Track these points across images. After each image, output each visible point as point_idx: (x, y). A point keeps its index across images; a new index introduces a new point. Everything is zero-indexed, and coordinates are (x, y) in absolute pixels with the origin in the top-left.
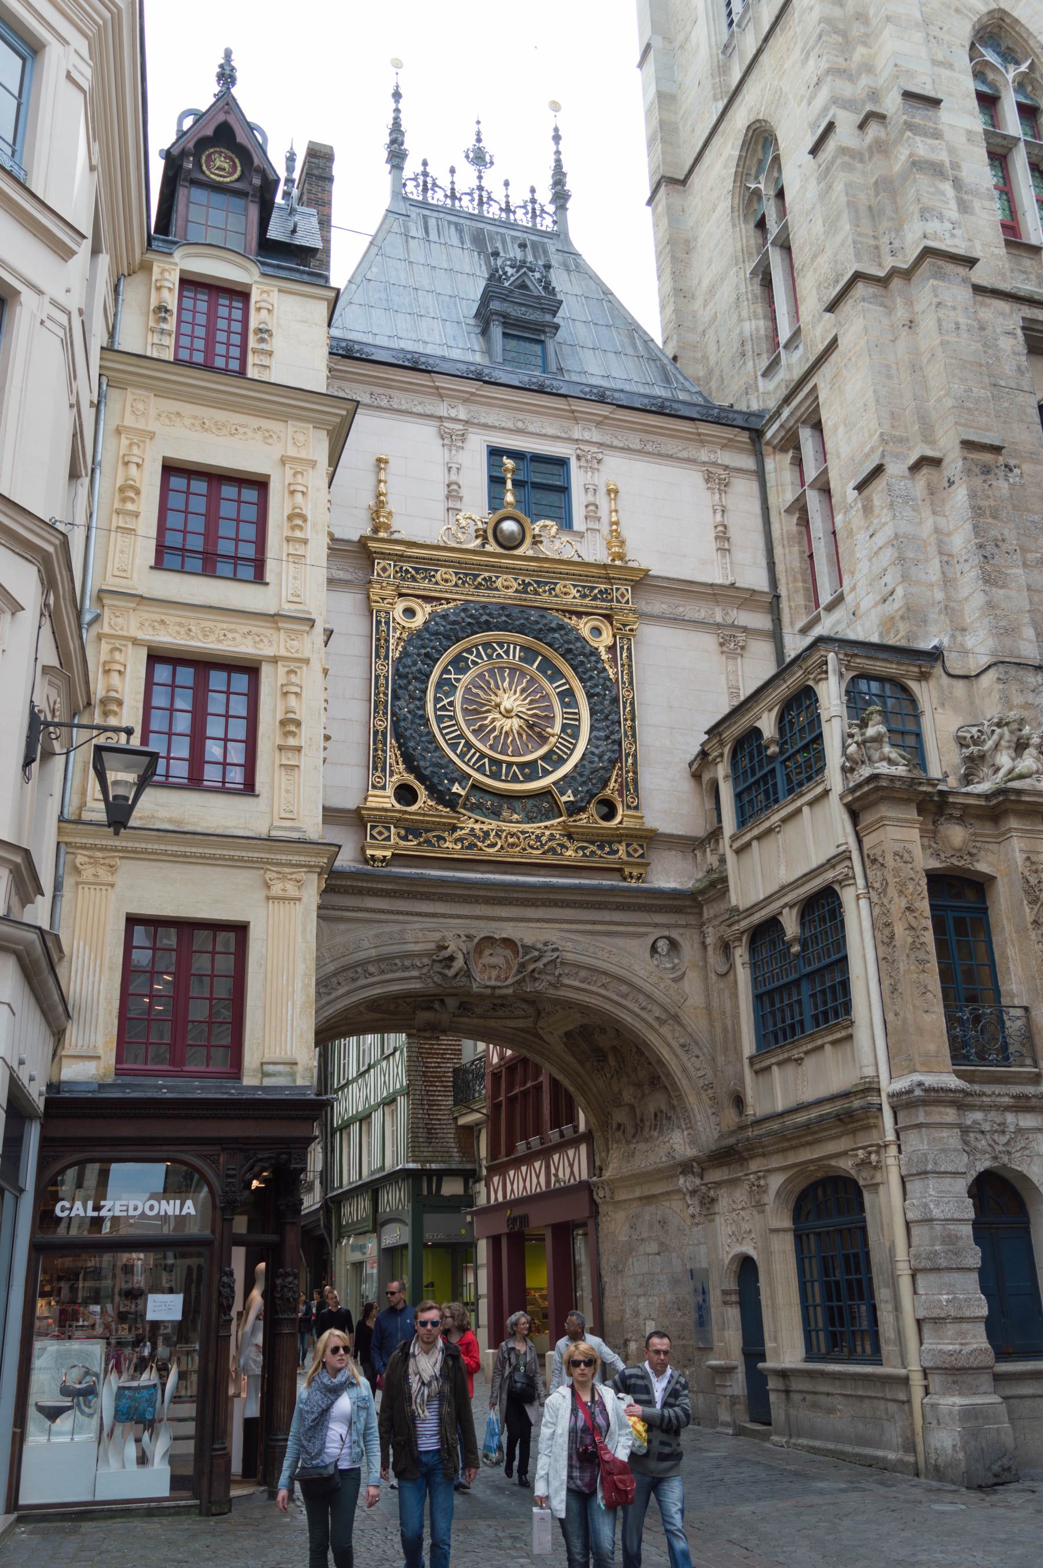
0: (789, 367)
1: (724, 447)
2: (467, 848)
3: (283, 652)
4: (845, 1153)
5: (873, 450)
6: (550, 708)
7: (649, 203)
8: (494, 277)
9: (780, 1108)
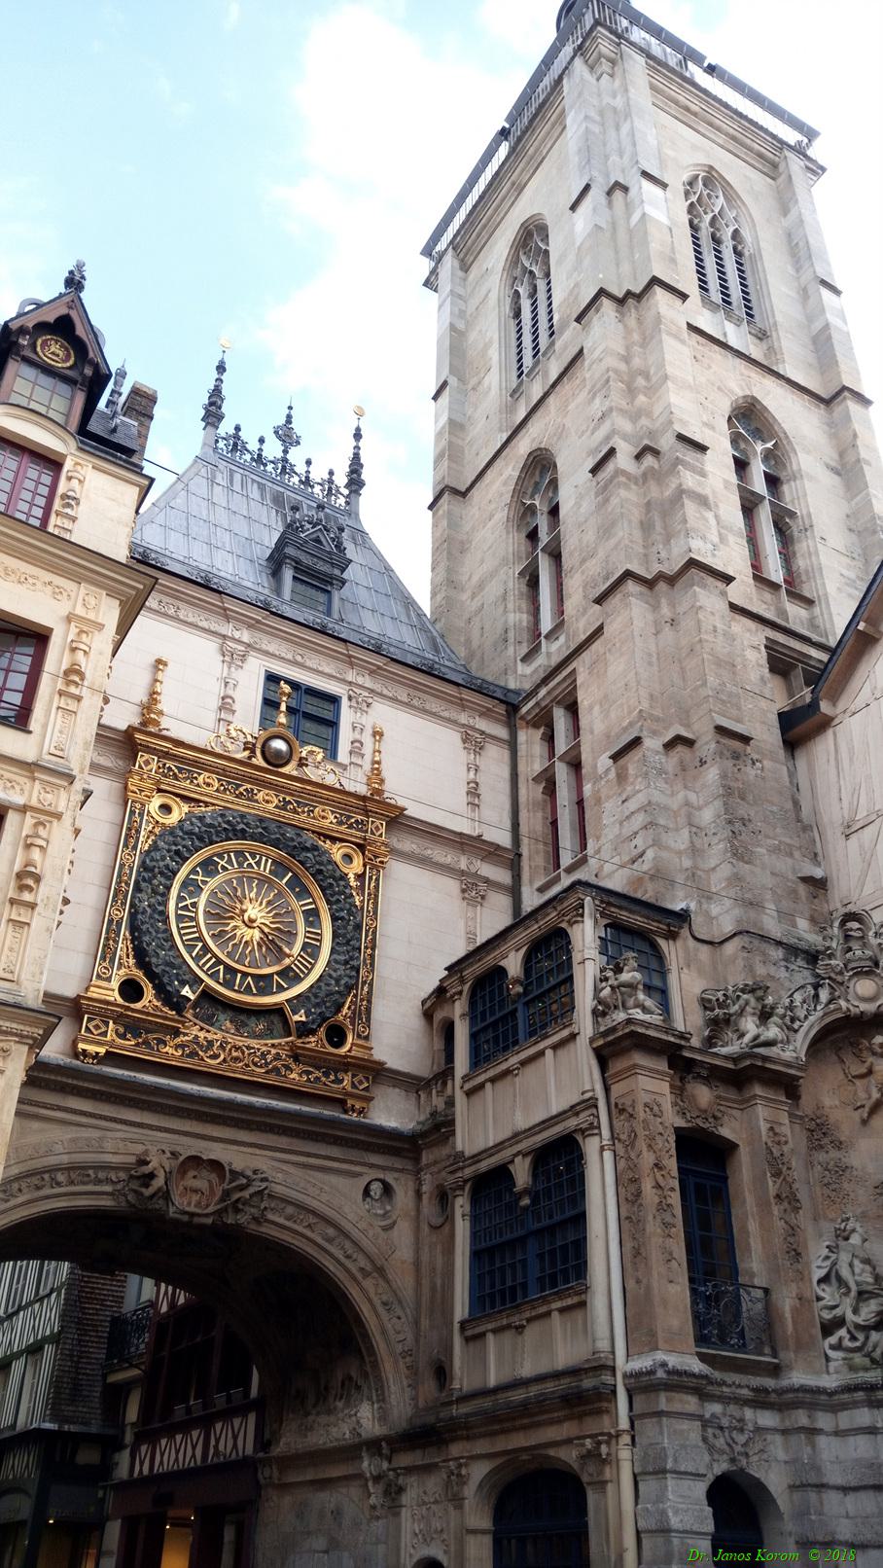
0: (549, 654)
1: (482, 715)
3: (34, 802)
4: (568, 1441)
5: (631, 724)
6: (294, 924)
7: (431, 507)
8: (291, 529)
9: (492, 1382)
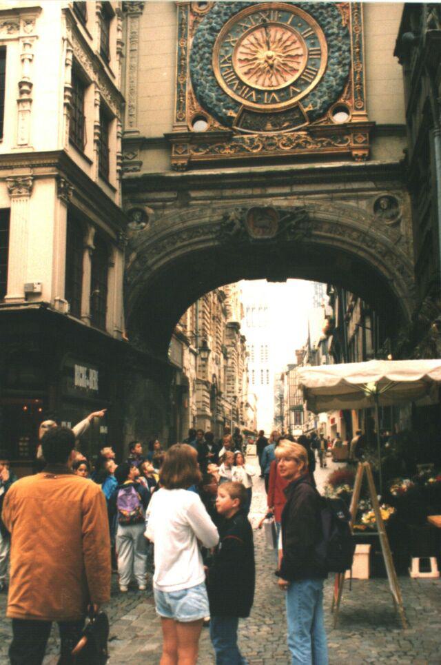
2: (239, 151)
